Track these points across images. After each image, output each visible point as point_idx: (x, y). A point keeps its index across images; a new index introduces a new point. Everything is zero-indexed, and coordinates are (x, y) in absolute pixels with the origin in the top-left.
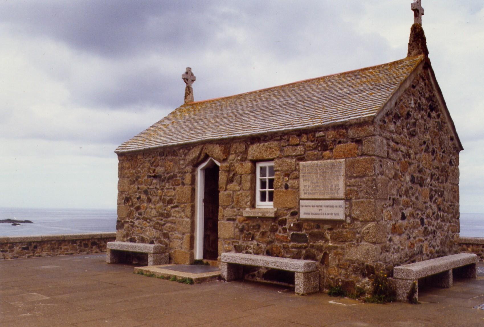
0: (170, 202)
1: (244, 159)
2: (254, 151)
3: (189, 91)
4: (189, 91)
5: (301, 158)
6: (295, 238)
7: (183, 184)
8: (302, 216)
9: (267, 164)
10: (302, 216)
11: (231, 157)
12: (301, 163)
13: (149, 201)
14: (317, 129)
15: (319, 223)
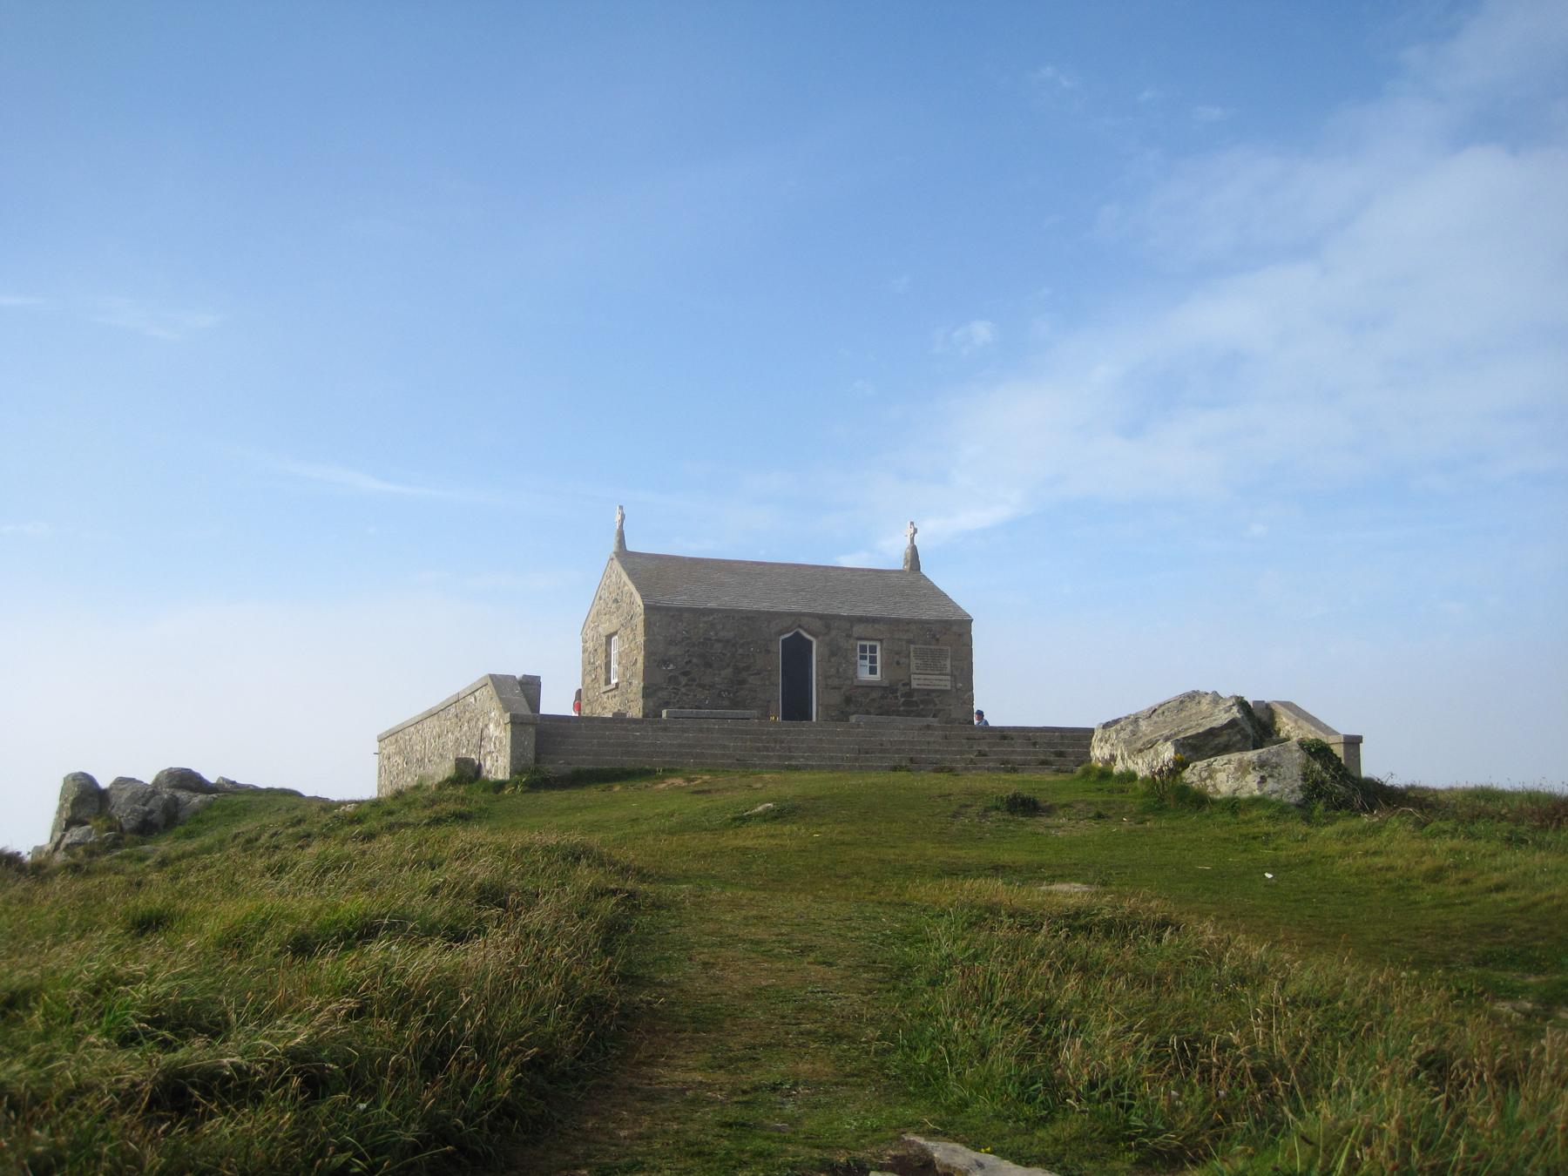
0: (747, 668)
1: (849, 636)
2: (858, 630)
3: (621, 535)
4: (621, 535)
5: (910, 642)
6: (904, 704)
7: (768, 652)
8: (914, 685)
9: (868, 643)
10: (914, 685)
11: (833, 633)
12: (912, 647)
13: (708, 665)
14: (927, 622)
15: (929, 692)
